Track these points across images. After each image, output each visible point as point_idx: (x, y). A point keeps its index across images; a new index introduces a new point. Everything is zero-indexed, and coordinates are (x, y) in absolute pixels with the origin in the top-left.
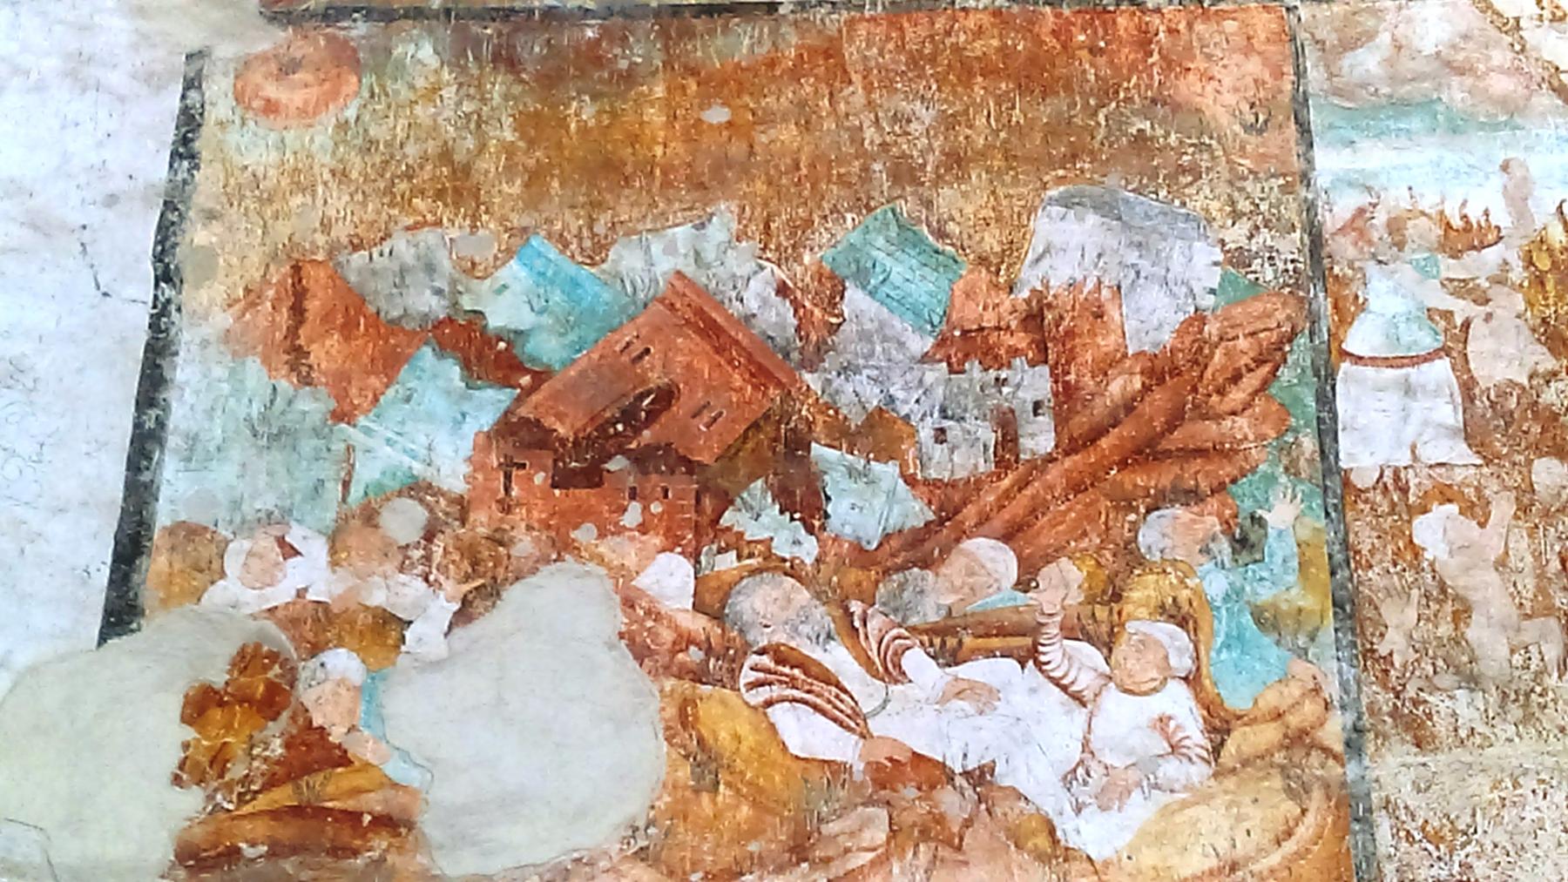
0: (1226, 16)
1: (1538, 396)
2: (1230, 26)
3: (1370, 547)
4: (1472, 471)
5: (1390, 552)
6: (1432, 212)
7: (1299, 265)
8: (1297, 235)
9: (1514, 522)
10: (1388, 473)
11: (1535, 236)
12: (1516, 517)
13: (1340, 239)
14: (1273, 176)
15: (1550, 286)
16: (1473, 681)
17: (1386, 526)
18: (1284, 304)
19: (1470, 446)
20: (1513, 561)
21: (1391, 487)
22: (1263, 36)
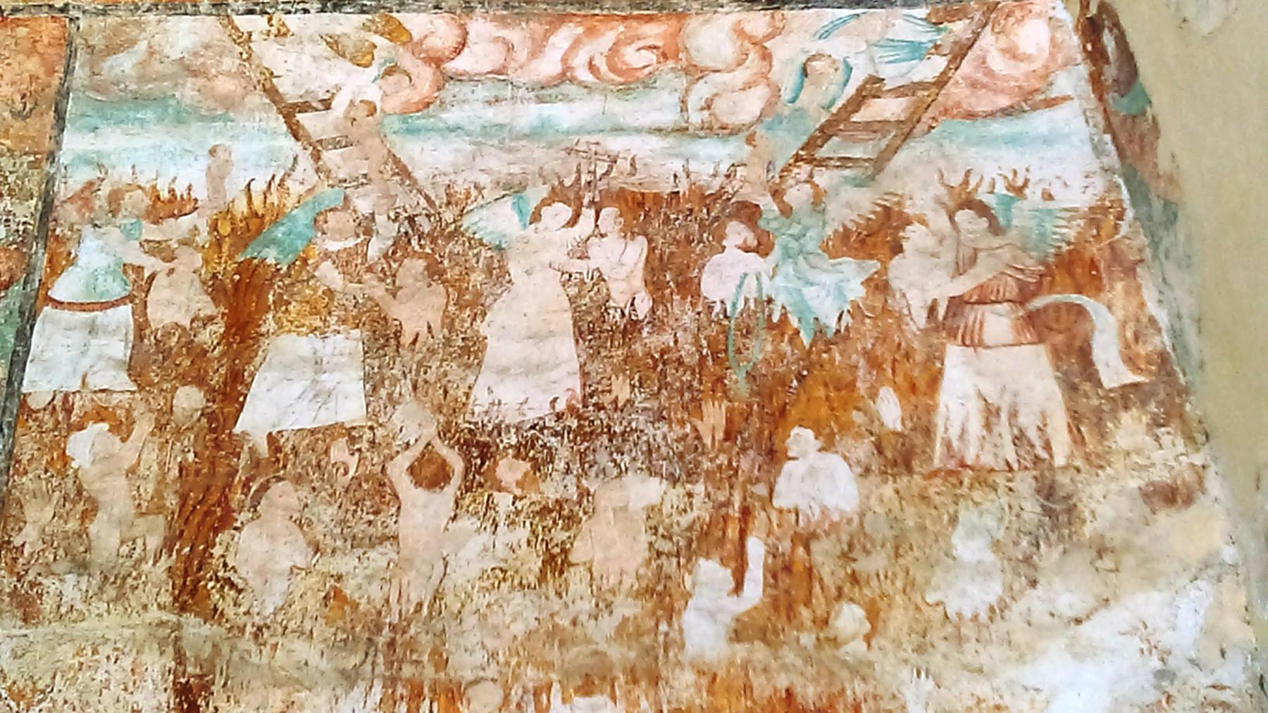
0: (20, 22)
1: (195, 336)
2: (22, 31)
3: (29, 457)
4: (128, 395)
5: (44, 462)
6: (148, 186)
7: (29, 227)
8: (33, 202)
9: (150, 438)
10: (59, 397)
11: (224, 208)
12: (153, 434)
13: (68, 206)
14: (26, 154)
15: (225, 248)
16: (82, 567)
17: (46, 440)
18: (8, 258)
19: (130, 375)
20: (142, 470)
21: (58, 409)
22: (46, 40)
